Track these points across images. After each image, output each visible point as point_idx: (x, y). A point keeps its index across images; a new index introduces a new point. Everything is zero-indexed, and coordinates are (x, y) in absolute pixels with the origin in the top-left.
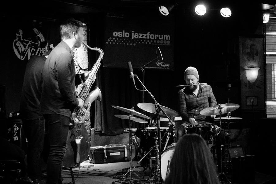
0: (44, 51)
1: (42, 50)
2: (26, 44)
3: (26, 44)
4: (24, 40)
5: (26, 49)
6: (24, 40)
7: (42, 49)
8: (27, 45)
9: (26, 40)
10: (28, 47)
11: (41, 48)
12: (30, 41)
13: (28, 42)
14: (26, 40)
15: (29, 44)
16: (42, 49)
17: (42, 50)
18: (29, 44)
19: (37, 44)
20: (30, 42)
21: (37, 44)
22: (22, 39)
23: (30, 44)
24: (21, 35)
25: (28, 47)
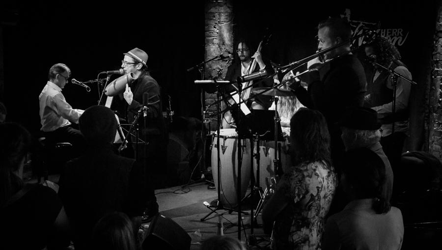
0: (388, 32)
1: (383, 31)
2: (355, 26)
3: (355, 26)
4: (353, 21)
5: (355, 33)
6: (353, 21)
7: (385, 30)
8: (355, 28)
9: (356, 22)
10: (359, 30)
11: (382, 30)
12: (361, 22)
13: (360, 23)
14: (356, 22)
15: (361, 25)
16: (385, 30)
17: (383, 31)
18: (361, 25)
19: (375, 24)
20: (363, 23)
21: (375, 24)
22: (349, 20)
23: (362, 26)
24: (348, 16)
25: (359, 30)
